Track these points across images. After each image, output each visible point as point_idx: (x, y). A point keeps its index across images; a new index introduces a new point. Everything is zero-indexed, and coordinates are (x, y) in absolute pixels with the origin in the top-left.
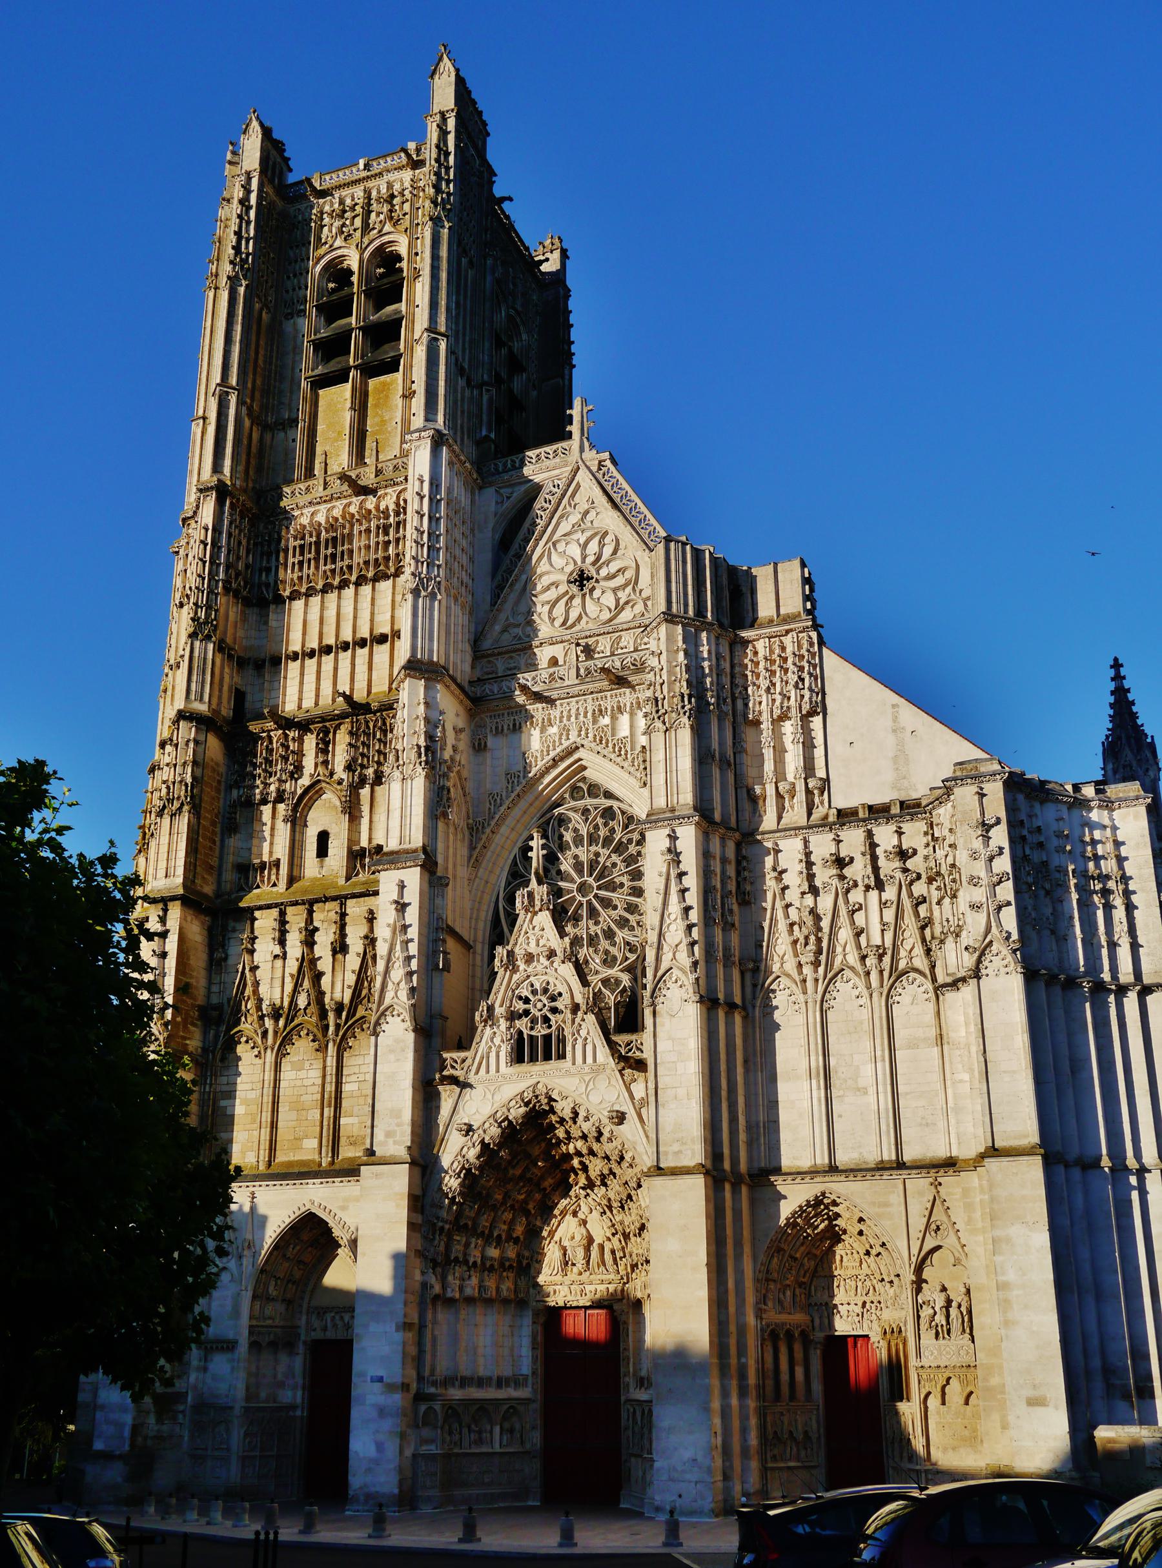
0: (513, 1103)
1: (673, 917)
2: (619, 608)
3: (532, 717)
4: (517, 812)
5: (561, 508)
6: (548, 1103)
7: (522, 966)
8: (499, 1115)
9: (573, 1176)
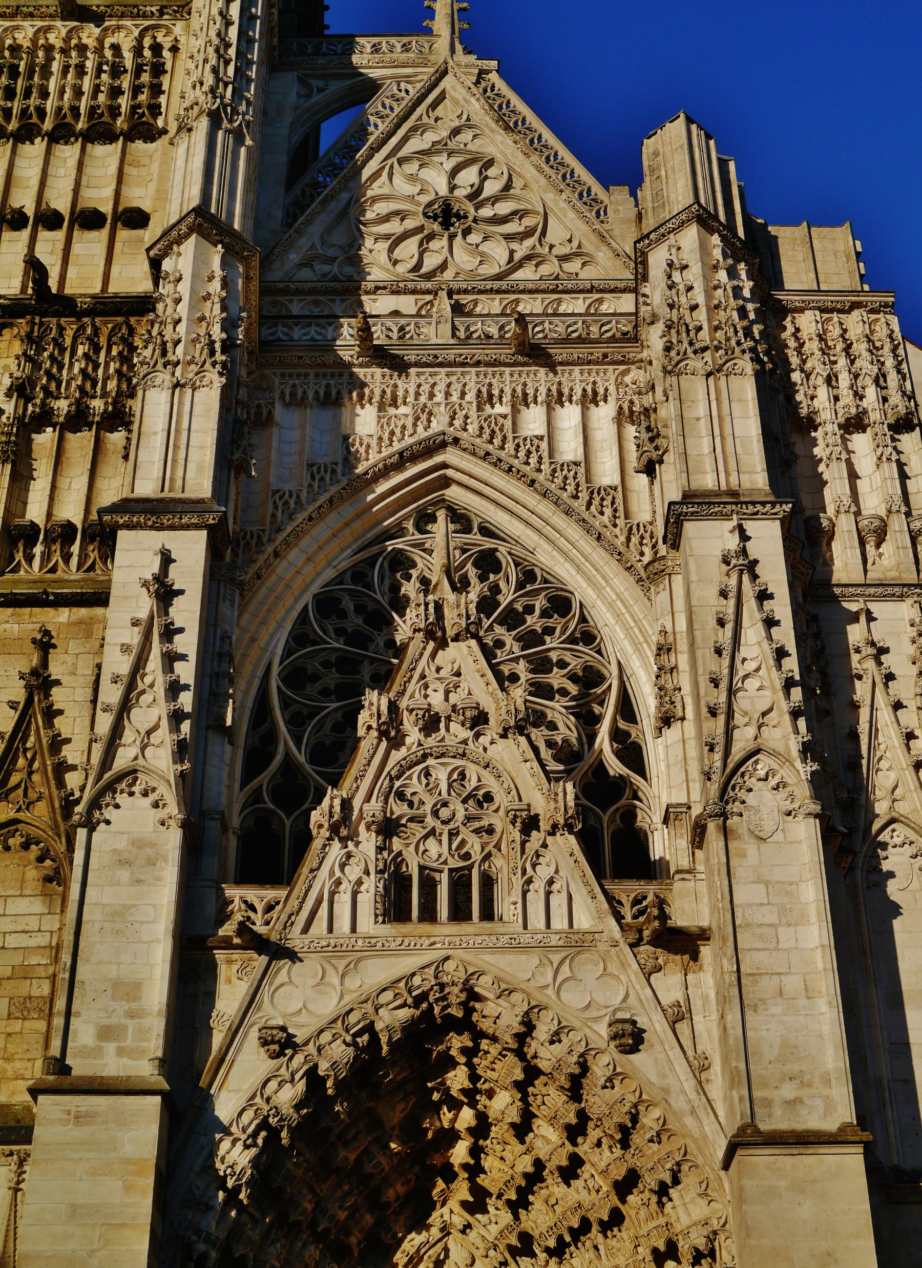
0: (388, 996)
1: (752, 666)
2: (515, 265)
3: (363, 385)
4: (321, 531)
5: (414, 117)
6: (464, 1005)
7: (413, 735)
8: (353, 1018)
9: (441, 1185)
